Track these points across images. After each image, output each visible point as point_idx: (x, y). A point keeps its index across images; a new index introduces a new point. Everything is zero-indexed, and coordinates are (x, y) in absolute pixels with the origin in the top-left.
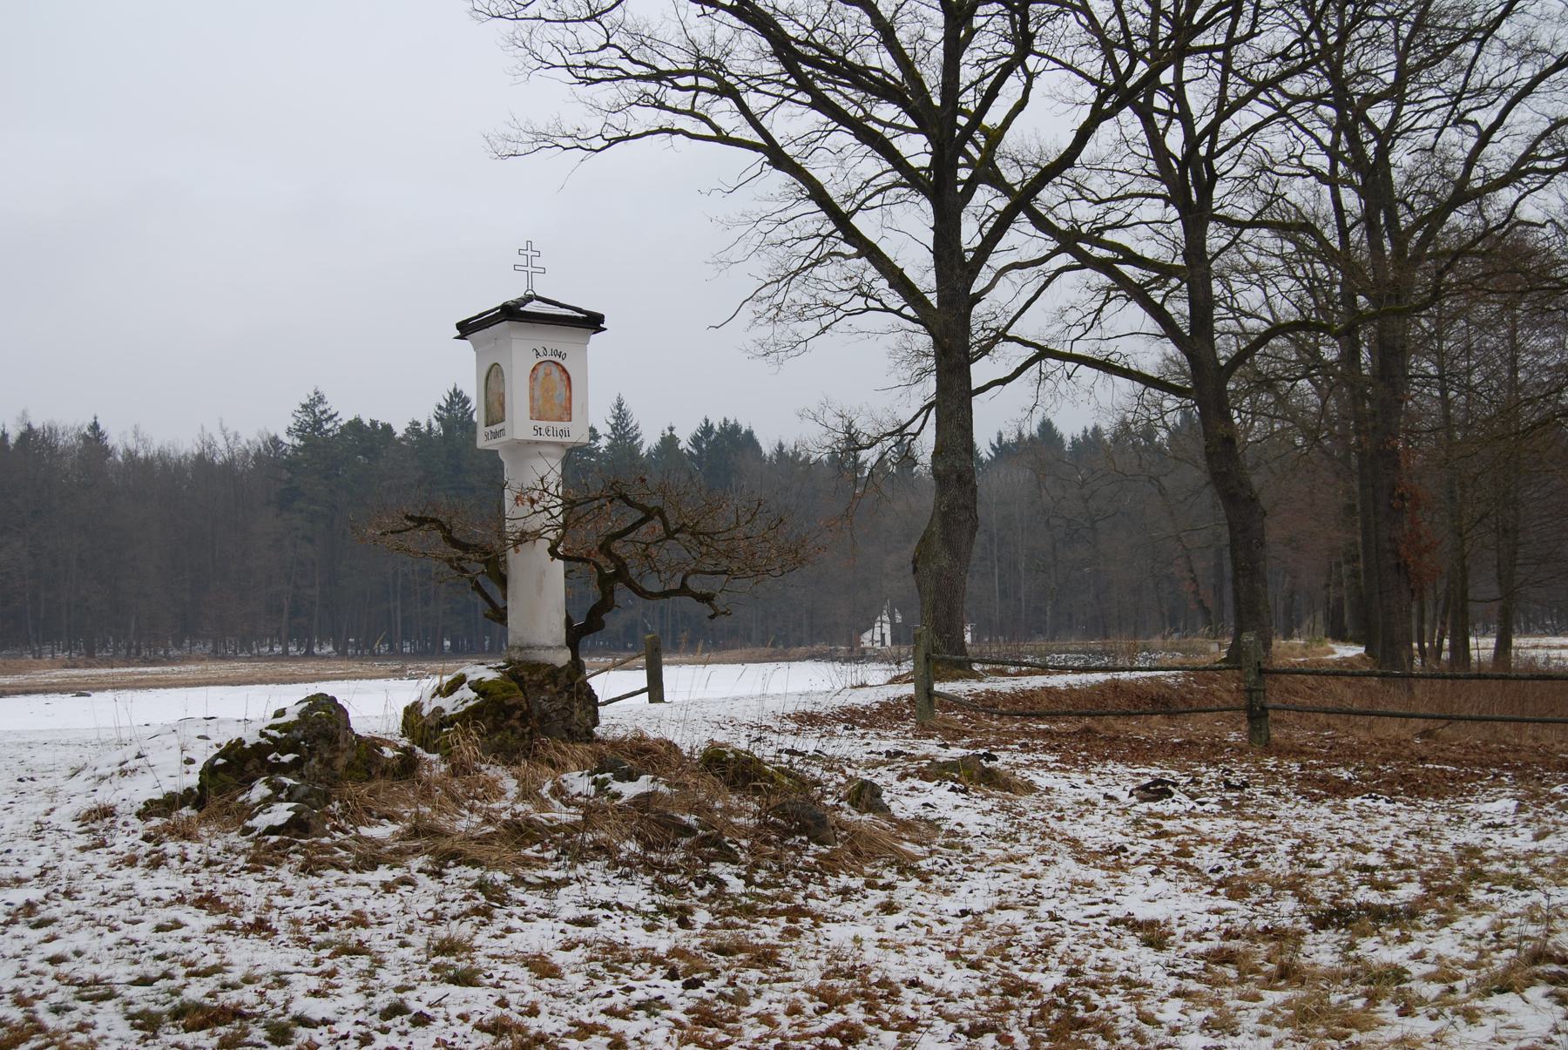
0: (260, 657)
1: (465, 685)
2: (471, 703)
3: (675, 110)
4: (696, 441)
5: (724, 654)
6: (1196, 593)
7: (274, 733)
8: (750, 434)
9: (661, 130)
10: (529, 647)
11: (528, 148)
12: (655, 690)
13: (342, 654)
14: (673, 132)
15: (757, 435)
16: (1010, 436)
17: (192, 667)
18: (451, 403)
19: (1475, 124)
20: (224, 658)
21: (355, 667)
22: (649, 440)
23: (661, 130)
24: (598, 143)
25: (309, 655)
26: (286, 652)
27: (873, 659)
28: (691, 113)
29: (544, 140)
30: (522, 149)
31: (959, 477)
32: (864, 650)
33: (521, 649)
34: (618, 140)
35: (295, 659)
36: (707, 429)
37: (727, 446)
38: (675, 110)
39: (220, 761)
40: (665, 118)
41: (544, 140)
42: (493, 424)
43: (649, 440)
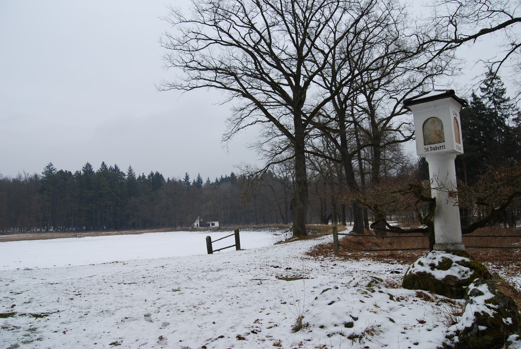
0: (34, 232)
1: (454, 264)
2: (471, 273)
3: (210, 81)
4: (149, 177)
5: (159, 230)
6: (281, 213)
7: (491, 305)
8: (161, 175)
9: (207, 85)
10: (457, 244)
11: (168, 88)
12: (238, 245)
13: (57, 231)
14: (211, 86)
15: (163, 176)
16: (224, 177)
17: (15, 235)
18: (87, 166)
19: (396, 98)
20: (24, 233)
21: (62, 235)
22: (137, 177)
23: (207, 85)
24: (189, 88)
25: (47, 231)
26: (41, 231)
27: (197, 230)
28: (215, 81)
29: (174, 86)
30: (166, 88)
31: (305, 182)
32: (196, 228)
33: (453, 244)
34: (194, 88)
35: (43, 232)
36: (152, 174)
37: (157, 178)
38: (210, 81)
39: (482, 328)
40: (207, 82)
41: (174, 86)
42: (430, 143)
43: (137, 177)
